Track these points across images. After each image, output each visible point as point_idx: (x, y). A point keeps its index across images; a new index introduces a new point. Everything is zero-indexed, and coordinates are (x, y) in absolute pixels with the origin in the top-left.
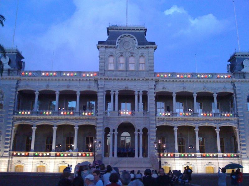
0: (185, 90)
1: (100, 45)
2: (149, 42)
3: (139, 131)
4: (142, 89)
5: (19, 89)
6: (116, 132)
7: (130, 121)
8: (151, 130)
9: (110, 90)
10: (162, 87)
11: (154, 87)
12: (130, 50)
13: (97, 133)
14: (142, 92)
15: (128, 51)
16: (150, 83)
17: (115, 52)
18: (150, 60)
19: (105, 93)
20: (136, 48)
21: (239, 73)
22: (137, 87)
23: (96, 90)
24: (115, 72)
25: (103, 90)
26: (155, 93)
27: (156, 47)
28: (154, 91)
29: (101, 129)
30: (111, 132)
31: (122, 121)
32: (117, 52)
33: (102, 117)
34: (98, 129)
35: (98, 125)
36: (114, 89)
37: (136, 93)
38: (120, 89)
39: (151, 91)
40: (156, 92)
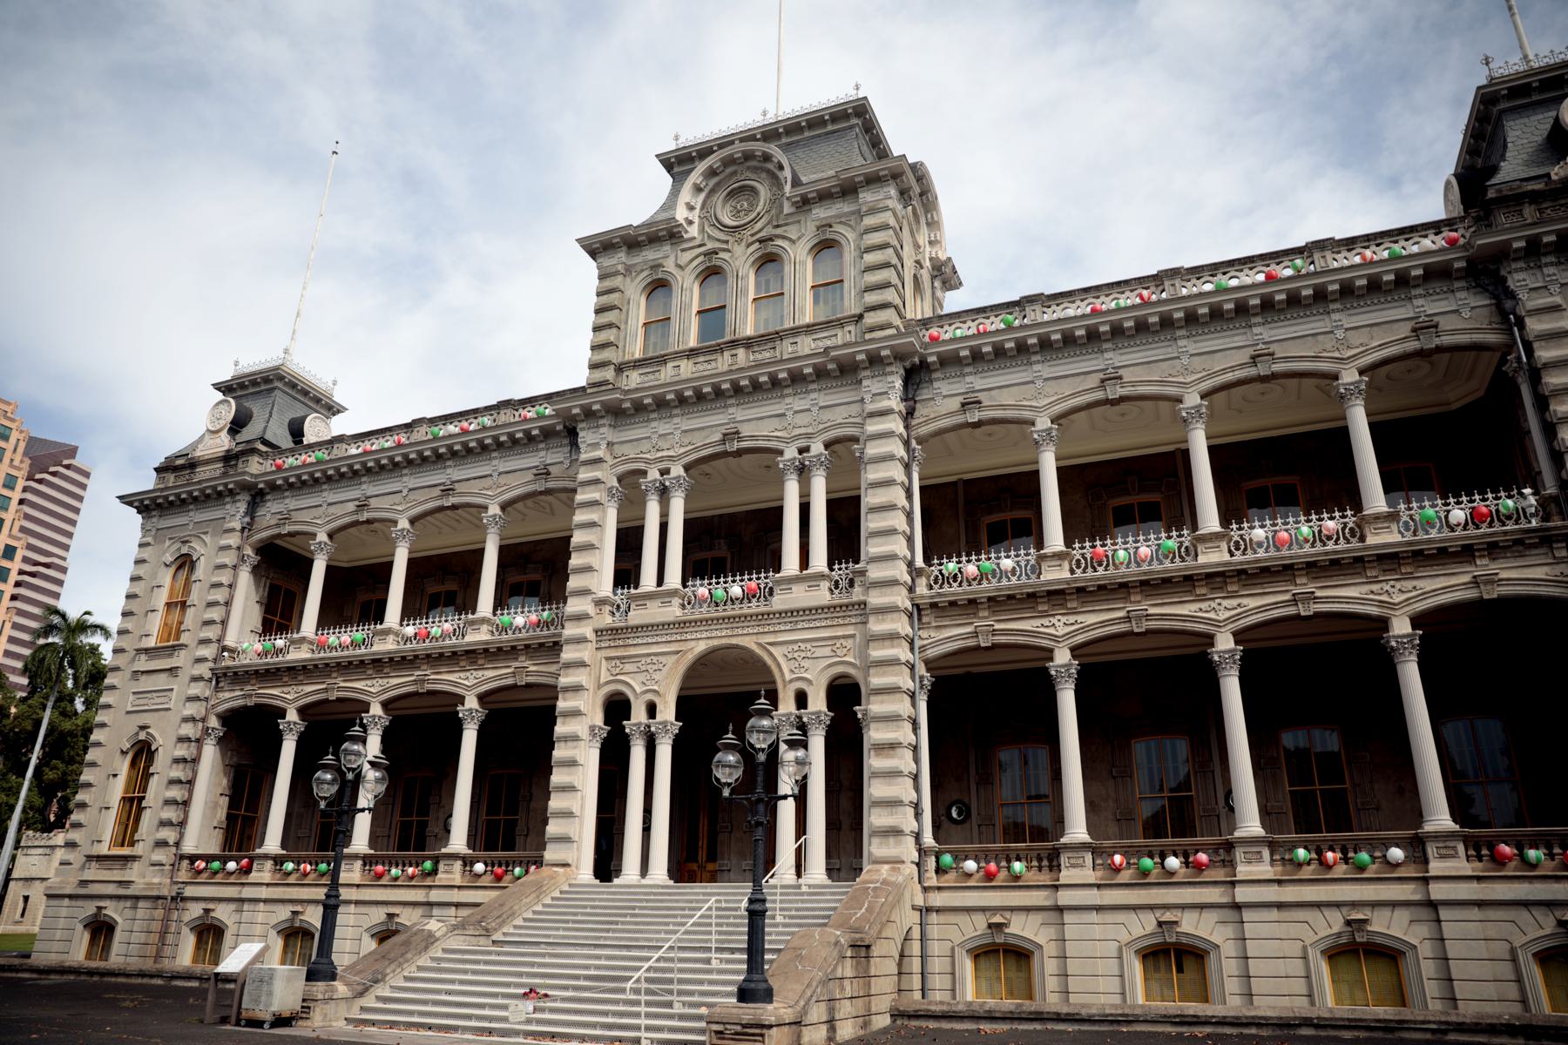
3: (801, 699)
9: (641, 466)
10: (954, 404)
12: (759, 225)
16: (865, 383)
18: (869, 249)
20: (787, 208)
24: (670, 365)
30: (639, 715)
31: (701, 647)
34: (562, 704)
36: (661, 459)
38: (697, 449)
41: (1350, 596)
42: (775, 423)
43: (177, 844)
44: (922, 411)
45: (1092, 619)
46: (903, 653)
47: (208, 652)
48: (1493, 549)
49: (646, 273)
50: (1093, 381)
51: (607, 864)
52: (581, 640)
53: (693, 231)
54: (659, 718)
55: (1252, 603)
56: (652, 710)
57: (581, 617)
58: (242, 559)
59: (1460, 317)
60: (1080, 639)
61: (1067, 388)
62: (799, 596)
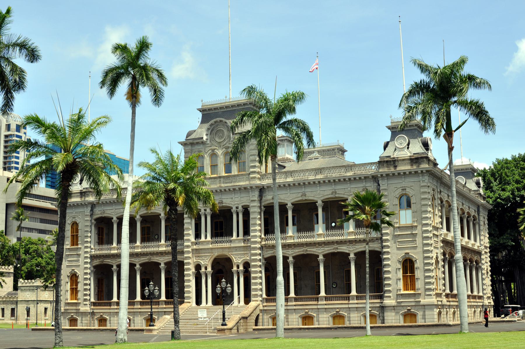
0: (304, 198)
4: (242, 203)
5: (95, 217)
6: (209, 269)
8: (253, 263)
12: (225, 142)
15: (222, 144)
16: (250, 193)
17: (205, 149)
18: (251, 155)
21: (387, 162)
22: (235, 202)
30: (203, 270)
32: (208, 149)
35: (185, 261)
37: (234, 210)
41: (344, 249)
42: (230, 200)
43: (90, 300)
44: (264, 198)
45: (297, 251)
46: (259, 257)
47: (89, 250)
49: (197, 152)
50: (300, 195)
51: (198, 302)
52: (188, 252)
53: (208, 142)
54: (208, 270)
55: (327, 249)
56: (206, 268)
57: (188, 246)
58: (92, 223)
59: (371, 187)
60: (294, 255)
61: (294, 196)
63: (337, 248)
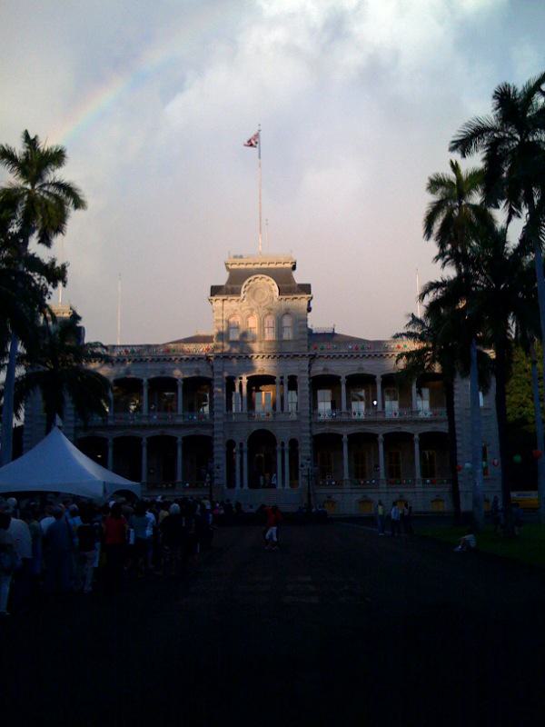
1: (214, 298)
2: (299, 285)
3: (283, 444)
7: (268, 427)
10: (322, 368)
11: (306, 368)
13: (215, 449)
14: (289, 377)
19: (225, 381)
23: (210, 376)
25: (220, 377)
26: (310, 378)
27: (312, 298)
28: (307, 375)
29: (221, 442)
30: (238, 447)
33: (221, 422)
37: (278, 380)
39: (303, 375)
40: (312, 375)
41: (407, 429)
46: (309, 434)
48: (436, 421)
56: (241, 445)
57: (218, 419)
62: (282, 417)
63: (400, 428)
